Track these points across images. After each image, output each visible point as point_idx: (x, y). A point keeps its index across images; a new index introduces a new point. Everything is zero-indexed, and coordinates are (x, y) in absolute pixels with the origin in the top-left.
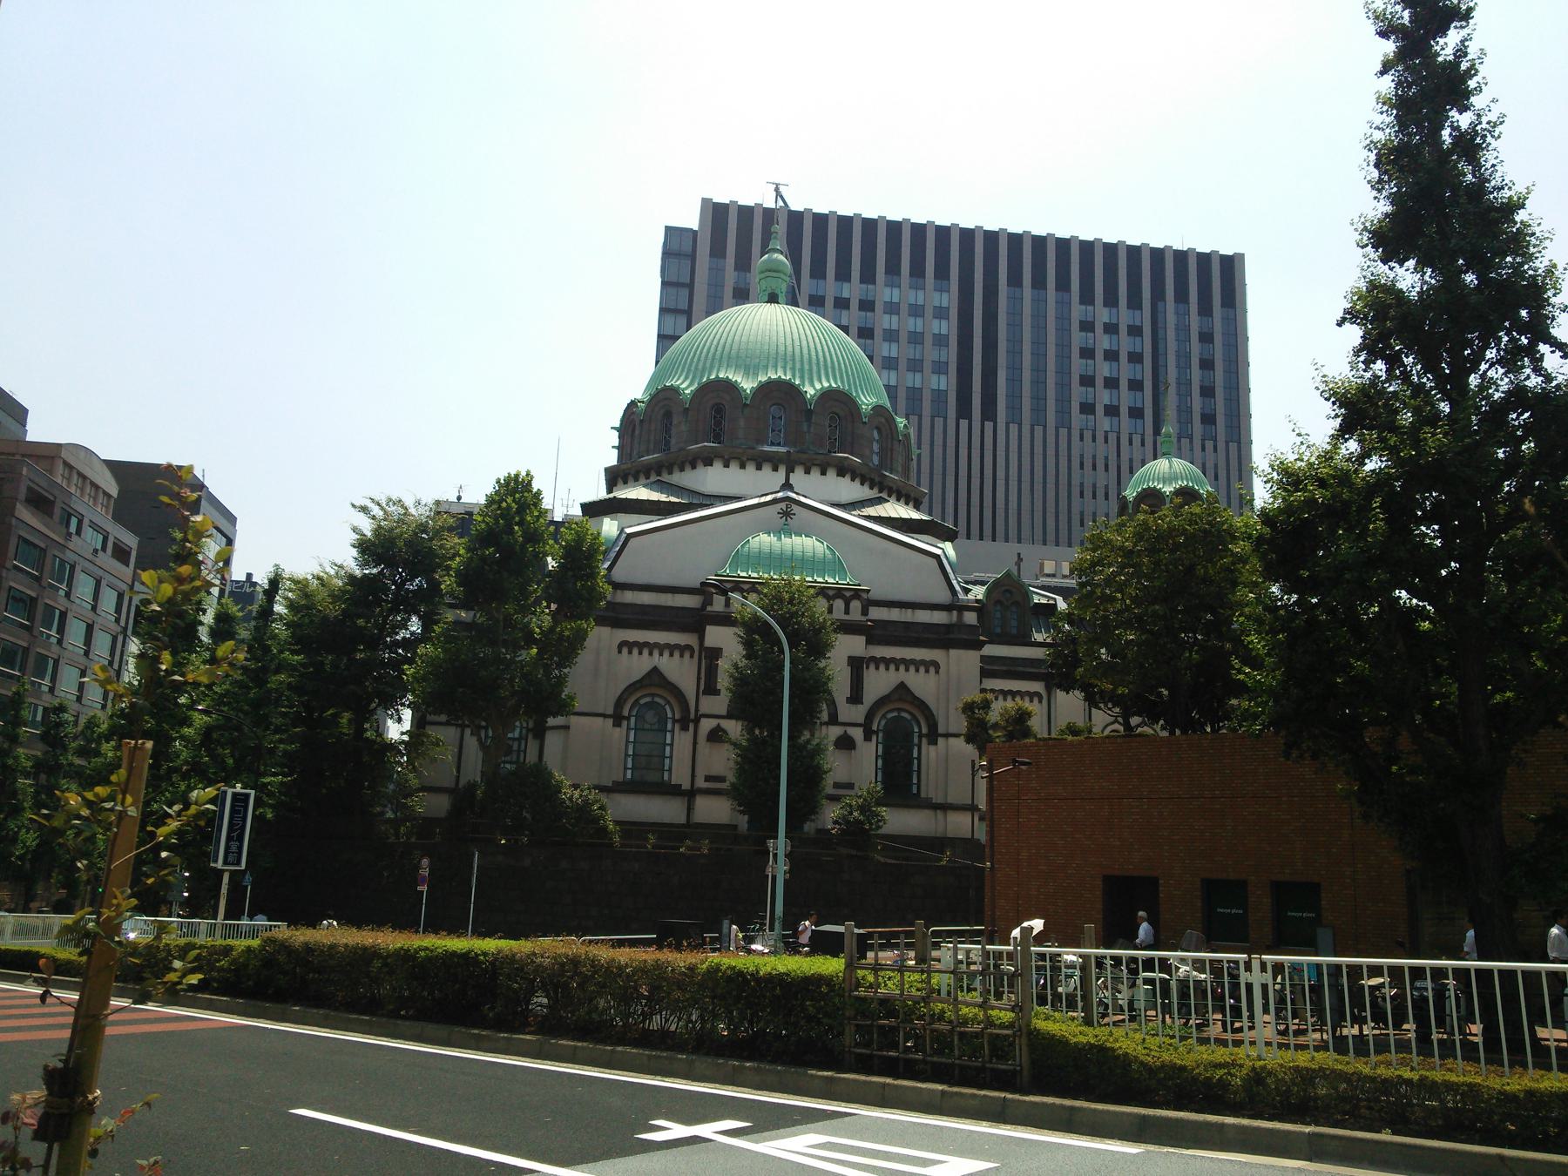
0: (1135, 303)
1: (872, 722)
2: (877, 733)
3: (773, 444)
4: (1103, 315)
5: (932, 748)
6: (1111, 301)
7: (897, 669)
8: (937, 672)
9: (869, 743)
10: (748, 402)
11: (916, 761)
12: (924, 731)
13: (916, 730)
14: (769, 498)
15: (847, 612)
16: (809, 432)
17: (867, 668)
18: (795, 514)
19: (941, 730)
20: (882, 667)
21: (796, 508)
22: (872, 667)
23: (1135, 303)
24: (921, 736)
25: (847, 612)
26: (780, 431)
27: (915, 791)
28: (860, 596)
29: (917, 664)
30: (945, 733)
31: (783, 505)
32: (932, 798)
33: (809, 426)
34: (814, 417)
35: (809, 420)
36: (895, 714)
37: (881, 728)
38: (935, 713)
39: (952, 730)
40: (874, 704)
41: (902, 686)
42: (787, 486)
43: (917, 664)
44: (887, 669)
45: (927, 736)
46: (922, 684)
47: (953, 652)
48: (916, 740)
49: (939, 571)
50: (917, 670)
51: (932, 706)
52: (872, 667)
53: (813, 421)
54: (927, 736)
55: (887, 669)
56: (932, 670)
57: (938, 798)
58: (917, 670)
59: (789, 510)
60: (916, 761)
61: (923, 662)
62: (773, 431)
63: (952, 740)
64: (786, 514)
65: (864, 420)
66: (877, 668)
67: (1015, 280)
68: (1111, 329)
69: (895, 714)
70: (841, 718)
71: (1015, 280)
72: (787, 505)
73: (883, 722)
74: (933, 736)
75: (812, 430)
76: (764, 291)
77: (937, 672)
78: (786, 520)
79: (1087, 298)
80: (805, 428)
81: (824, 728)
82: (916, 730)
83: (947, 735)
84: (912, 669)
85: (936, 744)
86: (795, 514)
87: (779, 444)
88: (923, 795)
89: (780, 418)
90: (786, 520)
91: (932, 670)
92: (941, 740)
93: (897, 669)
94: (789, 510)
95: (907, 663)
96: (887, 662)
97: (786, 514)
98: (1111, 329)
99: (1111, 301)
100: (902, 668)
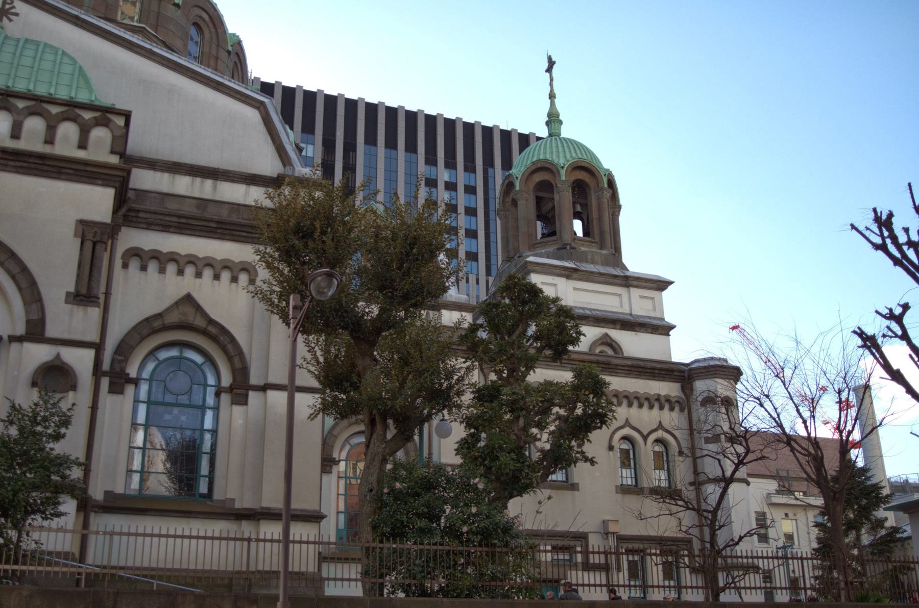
0: (470, 167)
1: (126, 360)
2: (136, 382)
4: (444, 175)
5: (237, 410)
6: (451, 164)
7: (181, 272)
9: (118, 397)
12: (226, 381)
13: (211, 380)
15: (83, 145)
17: (125, 266)
18: (17, 15)
19: (254, 380)
22: (134, 264)
23: (470, 167)
25: (83, 145)
27: (203, 488)
28: (110, 120)
29: (217, 267)
30: (262, 383)
32: (233, 500)
36: (174, 352)
37: (146, 374)
38: (245, 349)
39: (272, 380)
40: (134, 328)
44: (162, 271)
45: (230, 390)
49: (262, 128)
50: (217, 277)
51: (241, 337)
52: (134, 264)
55: (162, 271)
56: (243, 278)
57: (245, 502)
58: (217, 277)
66: (144, 268)
67: (371, 139)
68: (451, 186)
70: (52, 331)
71: (371, 139)
73: (150, 366)
79: (431, 160)
81: (15, 346)
82: (211, 380)
83: (264, 388)
84: (208, 273)
85: (245, 403)
86: (17, 15)
88: (217, 495)
91: (243, 278)
92: (253, 396)
93: (181, 272)
94: (7, 6)
95: (200, 265)
98: (451, 186)
99: (451, 164)
100: (190, 271)
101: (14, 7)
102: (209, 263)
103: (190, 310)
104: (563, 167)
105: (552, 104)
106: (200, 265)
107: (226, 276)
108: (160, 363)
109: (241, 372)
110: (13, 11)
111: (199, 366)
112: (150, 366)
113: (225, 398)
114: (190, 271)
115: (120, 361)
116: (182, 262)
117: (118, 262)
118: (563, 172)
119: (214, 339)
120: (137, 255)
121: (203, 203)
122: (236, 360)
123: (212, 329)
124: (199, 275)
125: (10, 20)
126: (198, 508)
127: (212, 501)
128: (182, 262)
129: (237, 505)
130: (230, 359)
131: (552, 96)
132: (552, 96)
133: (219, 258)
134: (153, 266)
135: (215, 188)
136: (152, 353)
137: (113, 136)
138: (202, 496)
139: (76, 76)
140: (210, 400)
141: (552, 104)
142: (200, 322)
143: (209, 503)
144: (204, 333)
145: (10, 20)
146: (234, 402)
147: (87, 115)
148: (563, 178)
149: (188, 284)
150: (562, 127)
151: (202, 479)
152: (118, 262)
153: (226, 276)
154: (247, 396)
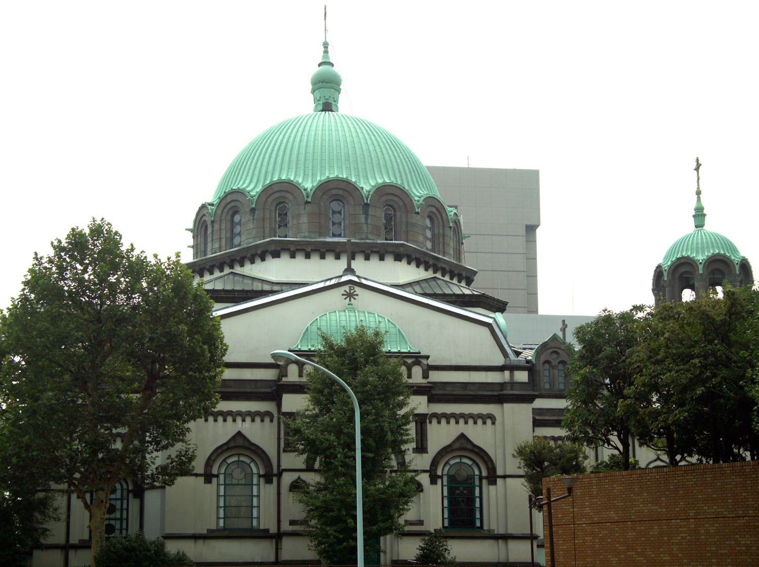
3: (334, 235)
5: (492, 488)
7: (457, 422)
8: (493, 423)
10: (309, 200)
11: (478, 500)
12: (484, 474)
13: (477, 472)
14: (333, 282)
16: (367, 223)
17: (430, 422)
18: (357, 295)
19: (500, 472)
20: (443, 421)
21: (358, 290)
22: (434, 421)
24: (481, 479)
26: (340, 224)
27: (478, 524)
29: (475, 418)
31: (347, 288)
32: (494, 530)
33: (366, 219)
34: (370, 209)
35: (366, 213)
36: (458, 460)
38: (493, 458)
41: (462, 436)
42: (349, 270)
43: (475, 418)
45: (487, 478)
46: (479, 435)
47: (506, 405)
48: (477, 482)
50: (475, 423)
51: (491, 453)
52: (434, 421)
53: (370, 213)
54: (487, 478)
55: (448, 423)
56: (489, 422)
58: (475, 423)
59: (352, 291)
60: (478, 500)
61: (480, 416)
62: (334, 224)
63: (508, 480)
64: (350, 295)
65: (417, 211)
66: (439, 422)
69: (458, 460)
72: (350, 287)
73: (447, 468)
74: (492, 478)
75: (369, 221)
76: (319, 100)
77: (493, 423)
78: (350, 300)
80: (363, 220)
83: (504, 477)
84: (471, 421)
86: (357, 295)
87: (340, 236)
88: (486, 527)
89: (340, 213)
90: (350, 300)
91: (489, 422)
92: (499, 481)
93: (457, 422)
94: (352, 291)
95: (466, 417)
96: (448, 417)
97: (350, 295)
100: (462, 421)
101: (355, 291)
102: (471, 416)
103: (464, 441)
104: (701, 263)
105: (699, 199)
106: (466, 417)
107: (480, 421)
108: (451, 466)
109: (492, 469)
110: (355, 293)
111: (470, 466)
112: (447, 468)
113: (484, 482)
114: (462, 421)
115: (434, 469)
116: (457, 417)
117: (428, 421)
118: (701, 267)
119: (477, 454)
120: (435, 416)
121: (465, 385)
122: (489, 464)
123: (475, 449)
124: (466, 423)
125: (355, 299)
126: (477, 535)
127: (483, 530)
128: (457, 417)
129: (496, 532)
130: (486, 463)
131: (698, 193)
132: (698, 193)
133: (476, 413)
134: (443, 421)
135: (470, 376)
136: (447, 463)
137: (423, 370)
138: (478, 528)
139: (398, 335)
140: (477, 482)
141: (699, 199)
142: (469, 446)
143: (482, 531)
144: (472, 451)
145: (355, 299)
146: (489, 484)
147: (409, 361)
148: (701, 272)
149: (461, 428)
150: (706, 217)
151: (477, 520)
152: (428, 421)
153: (480, 421)
154: (496, 481)
